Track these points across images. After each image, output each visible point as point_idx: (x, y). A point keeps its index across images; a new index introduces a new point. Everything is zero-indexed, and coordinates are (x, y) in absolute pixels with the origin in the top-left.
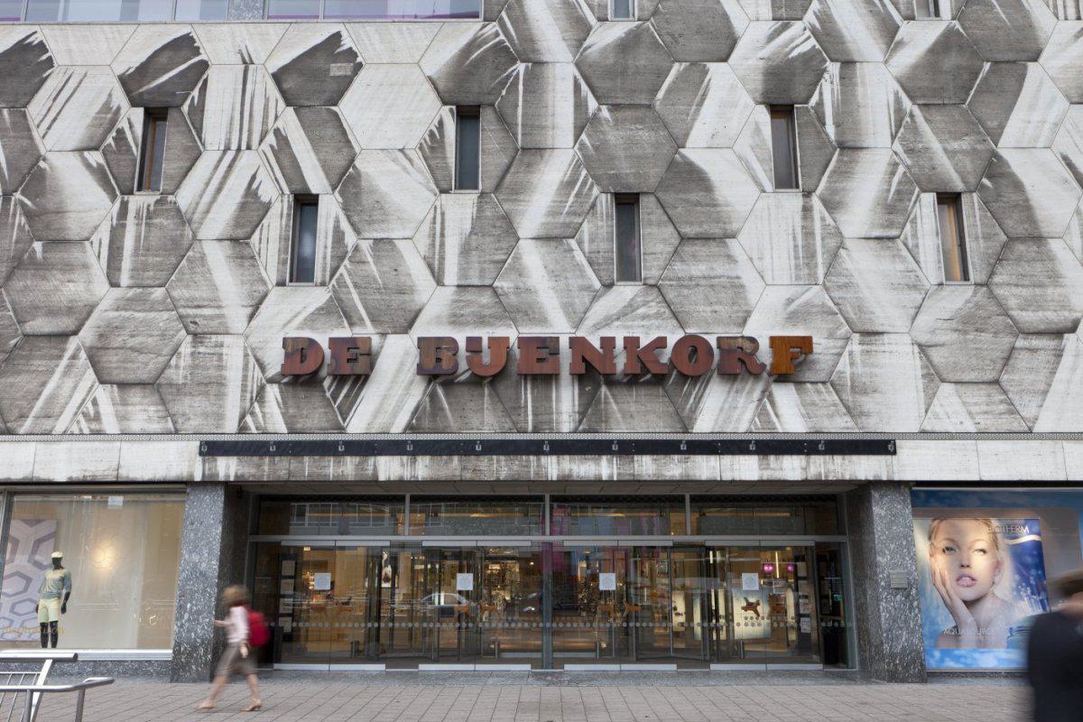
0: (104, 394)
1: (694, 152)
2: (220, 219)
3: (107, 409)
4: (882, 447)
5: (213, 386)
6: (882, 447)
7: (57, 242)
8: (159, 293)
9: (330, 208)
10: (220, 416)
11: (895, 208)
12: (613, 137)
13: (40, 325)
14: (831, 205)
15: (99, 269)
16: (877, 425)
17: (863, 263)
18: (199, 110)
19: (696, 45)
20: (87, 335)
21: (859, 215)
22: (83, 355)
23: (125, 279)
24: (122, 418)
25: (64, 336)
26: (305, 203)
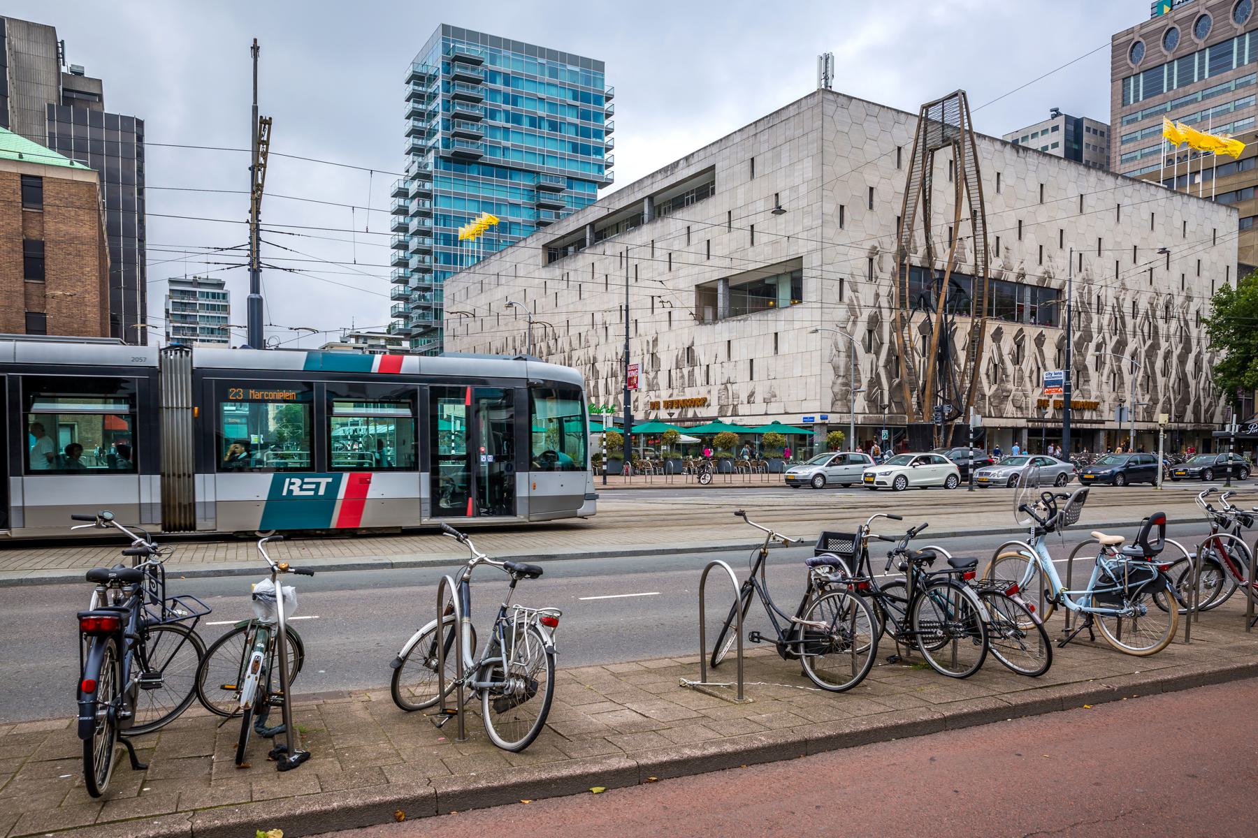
0: (1014, 409)
2: (1027, 374)
4: (1103, 422)
5: (1027, 408)
6: (1103, 422)
7: (1007, 376)
9: (1042, 369)
11: (1109, 377)
12: (1077, 358)
13: (1004, 394)
14: (1102, 375)
15: (1012, 382)
16: (1103, 419)
17: (1104, 386)
19: (1088, 338)
21: (1104, 379)
25: (1008, 396)
26: (1039, 369)
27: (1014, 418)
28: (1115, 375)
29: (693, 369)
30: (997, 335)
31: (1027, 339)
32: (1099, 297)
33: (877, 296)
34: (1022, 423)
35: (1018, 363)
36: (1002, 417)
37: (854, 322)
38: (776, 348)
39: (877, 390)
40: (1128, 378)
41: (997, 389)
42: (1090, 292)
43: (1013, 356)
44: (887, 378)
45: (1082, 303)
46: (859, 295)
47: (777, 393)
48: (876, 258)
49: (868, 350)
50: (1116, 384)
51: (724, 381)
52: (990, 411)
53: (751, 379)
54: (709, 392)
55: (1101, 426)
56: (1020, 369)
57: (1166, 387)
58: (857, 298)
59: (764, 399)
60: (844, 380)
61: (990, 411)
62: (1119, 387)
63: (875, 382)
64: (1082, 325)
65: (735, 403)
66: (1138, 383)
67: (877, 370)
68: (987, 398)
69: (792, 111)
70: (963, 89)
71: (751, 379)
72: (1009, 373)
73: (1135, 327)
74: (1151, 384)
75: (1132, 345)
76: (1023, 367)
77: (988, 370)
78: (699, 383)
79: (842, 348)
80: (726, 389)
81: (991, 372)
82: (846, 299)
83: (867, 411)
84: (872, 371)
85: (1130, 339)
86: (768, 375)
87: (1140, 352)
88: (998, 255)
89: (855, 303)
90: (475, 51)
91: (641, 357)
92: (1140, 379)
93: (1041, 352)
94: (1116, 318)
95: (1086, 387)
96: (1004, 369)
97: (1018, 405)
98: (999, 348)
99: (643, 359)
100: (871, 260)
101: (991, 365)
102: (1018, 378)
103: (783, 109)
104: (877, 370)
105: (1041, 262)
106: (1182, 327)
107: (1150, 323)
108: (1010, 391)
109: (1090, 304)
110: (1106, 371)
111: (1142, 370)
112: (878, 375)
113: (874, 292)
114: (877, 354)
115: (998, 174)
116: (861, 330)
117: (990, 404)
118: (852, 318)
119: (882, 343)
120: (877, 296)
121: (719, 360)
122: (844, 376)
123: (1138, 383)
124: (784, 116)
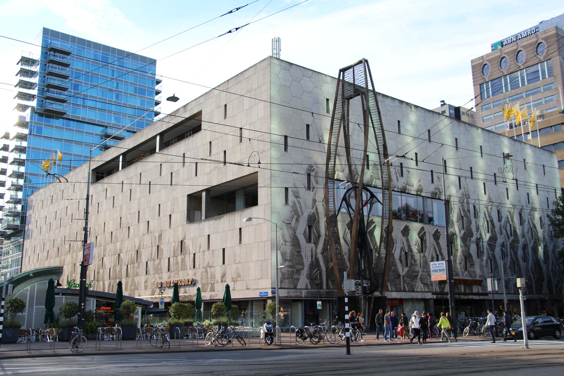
0: (422, 285)
1: (471, 252)
3: (423, 288)
7: (415, 261)
8: (425, 270)
10: (433, 289)
13: (414, 274)
14: (482, 261)
18: (426, 240)
20: (419, 277)
21: (484, 263)
22: (419, 280)
23: (422, 268)
24: (424, 289)
27: (422, 292)
28: (491, 260)
29: (185, 257)
30: (406, 232)
31: (427, 234)
32: (474, 206)
33: (314, 201)
34: (429, 296)
35: (422, 252)
36: (413, 291)
37: (297, 220)
38: (240, 240)
39: (317, 271)
40: (501, 263)
41: (409, 271)
42: (468, 203)
43: (418, 246)
44: (324, 262)
45: (464, 210)
46: (300, 200)
47: (241, 274)
48: (313, 174)
49: (309, 241)
50: (493, 268)
51: (205, 265)
52: (404, 287)
53: (224, 263)
54: (195, 274)
55: (486, 297)
56: (424, 256)
57: (527, 269)
58: (299, 202)
59: (233, 278)
60: (290, 263)
61: (404, 287)
62: (495, 269)
63: (315, 264)
64: (465, 226)
65: (213, 282)
66: (508, 266)
67: (316, 256)
68: (402, 277)
69: (251, 72)
70: (366, 58)
71: (224, 263)
72: (416, 259)
73: (501, 228)
74: (516, 267)
75: (500, 241)
76: (426, 254)
77: (401, 256)
78: (188, 267)
79: (288, 239)
80: (206, 271)
81: (403, 258)
82: (290, 202)
83: (309, 287)
84: (312, 256)
85: (498, 236)
86: (235, 260)
87: (506, 245)
88: (402, 175)
89: (298, 205)
90: (66, 47)
91: (150, 248)
92: (508, 263)
93: (438, 244)
94: (488, 221)
95: (472, 269)
96: (413, 256)
97: (425, 282)
98: (408, 241)
99: (152, 250)
100: (309, 175)
101: (403, 253)
102: (423, 263)
103: (246, 70)
104: (316, 256)
105: (433, 182)
106: (532, 228)
107: (511, 225)
108: (418, 272)
109: (469, 211)
110: (485, 258)
111: (509, 257)
112: (317, 260)
113: (311, 198)
114: (316, 243)
115: (399, 122)
116: (302, 226)
117: (404, 281)
118: (296, 216)
119: (319, 236)
120: (314, 201)
121: (202, 250)
122: (290, 260)
123: (508, 266)
124: (246, 75)
